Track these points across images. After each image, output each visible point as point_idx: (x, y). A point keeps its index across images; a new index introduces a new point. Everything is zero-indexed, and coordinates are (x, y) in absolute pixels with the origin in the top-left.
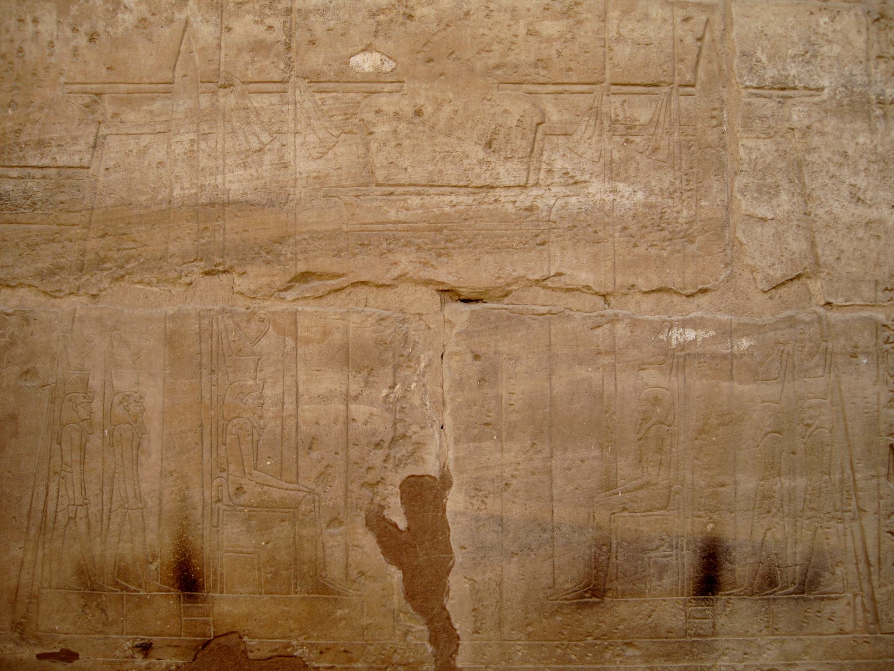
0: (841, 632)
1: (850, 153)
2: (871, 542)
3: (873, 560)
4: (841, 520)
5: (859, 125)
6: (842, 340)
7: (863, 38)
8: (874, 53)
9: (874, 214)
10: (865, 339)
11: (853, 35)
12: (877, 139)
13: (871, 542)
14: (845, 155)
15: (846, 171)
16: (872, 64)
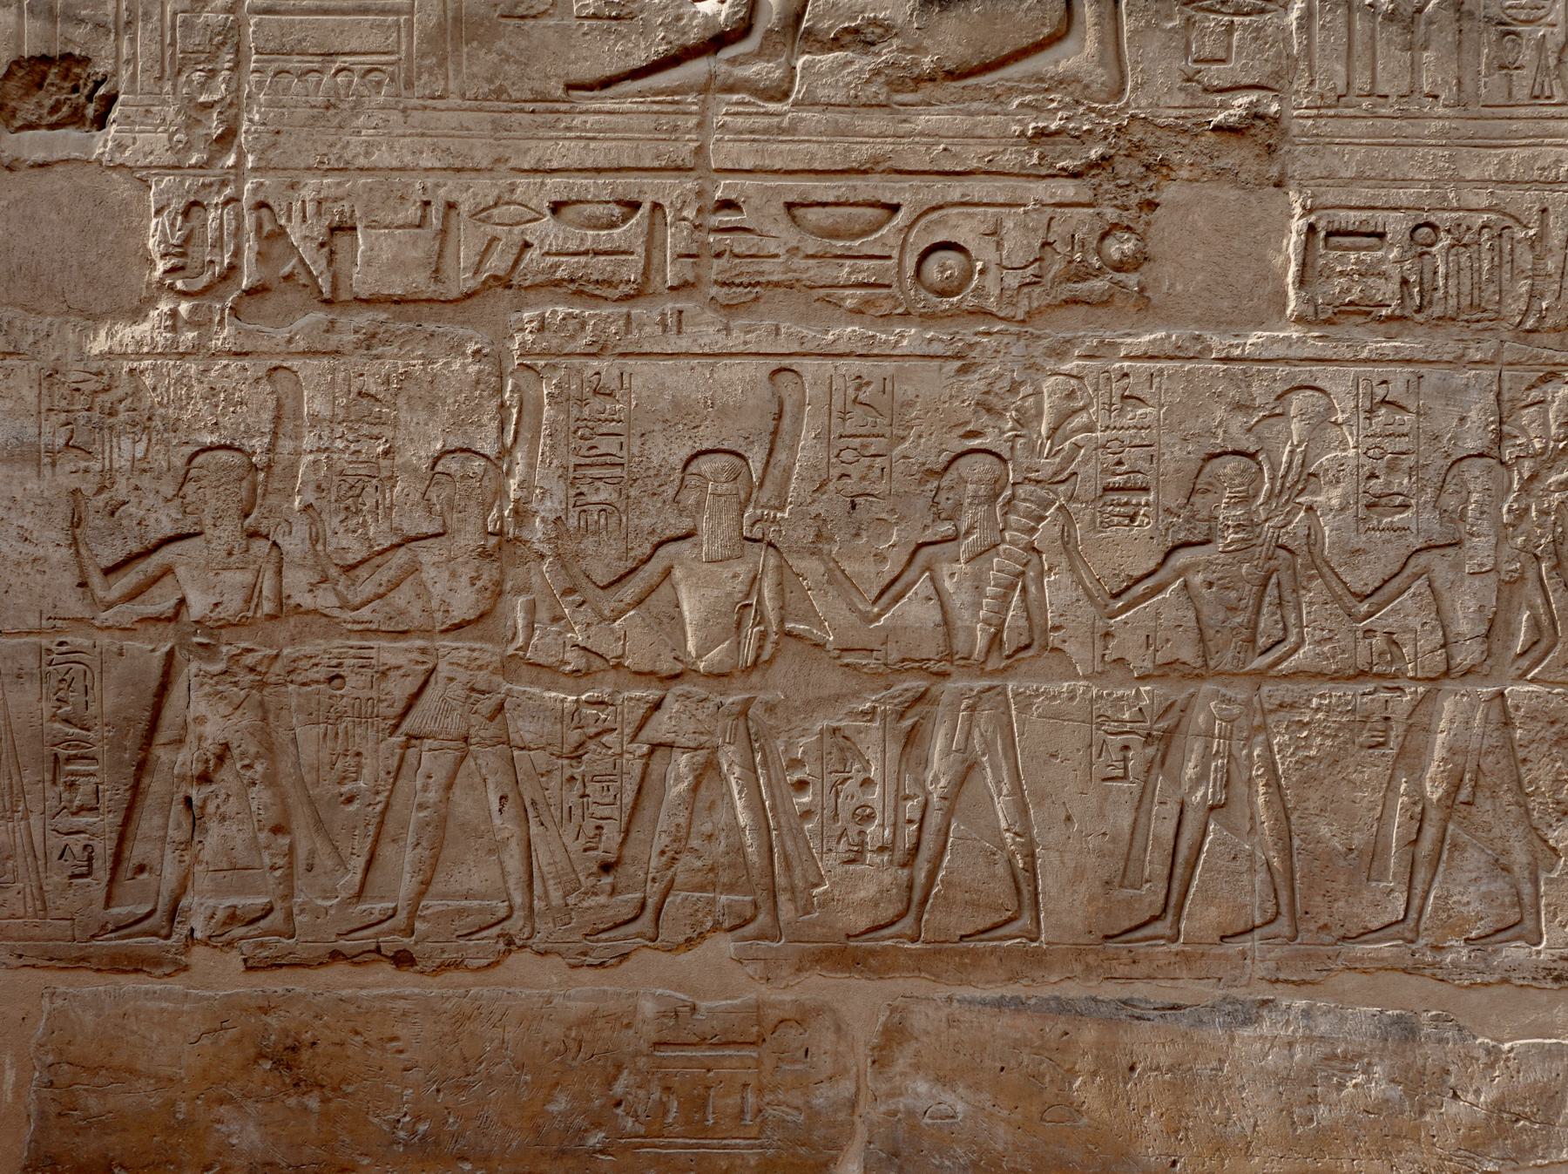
0: (12, 916)
1: (18, 498)
2: (38, 839)
3: (40, 854)
4: (11, 819)
5: (29, 471)
6: (9, 663)
7: (36, 391)
8: (45, 406)
9: (41, 552)
10: (30, 662)
11: (25, 391)
12: (45, 485)
13: (38, 839)
14: (14, 499)
15: (13, 514)
16: (43, 416)
